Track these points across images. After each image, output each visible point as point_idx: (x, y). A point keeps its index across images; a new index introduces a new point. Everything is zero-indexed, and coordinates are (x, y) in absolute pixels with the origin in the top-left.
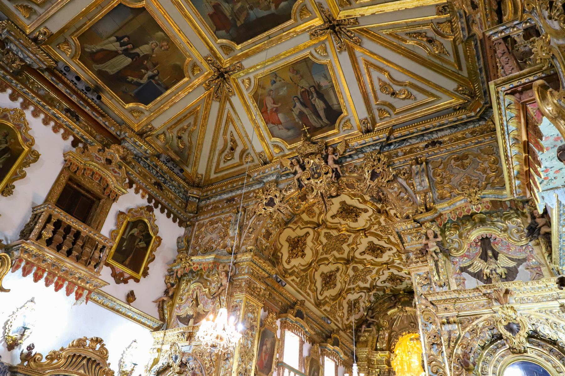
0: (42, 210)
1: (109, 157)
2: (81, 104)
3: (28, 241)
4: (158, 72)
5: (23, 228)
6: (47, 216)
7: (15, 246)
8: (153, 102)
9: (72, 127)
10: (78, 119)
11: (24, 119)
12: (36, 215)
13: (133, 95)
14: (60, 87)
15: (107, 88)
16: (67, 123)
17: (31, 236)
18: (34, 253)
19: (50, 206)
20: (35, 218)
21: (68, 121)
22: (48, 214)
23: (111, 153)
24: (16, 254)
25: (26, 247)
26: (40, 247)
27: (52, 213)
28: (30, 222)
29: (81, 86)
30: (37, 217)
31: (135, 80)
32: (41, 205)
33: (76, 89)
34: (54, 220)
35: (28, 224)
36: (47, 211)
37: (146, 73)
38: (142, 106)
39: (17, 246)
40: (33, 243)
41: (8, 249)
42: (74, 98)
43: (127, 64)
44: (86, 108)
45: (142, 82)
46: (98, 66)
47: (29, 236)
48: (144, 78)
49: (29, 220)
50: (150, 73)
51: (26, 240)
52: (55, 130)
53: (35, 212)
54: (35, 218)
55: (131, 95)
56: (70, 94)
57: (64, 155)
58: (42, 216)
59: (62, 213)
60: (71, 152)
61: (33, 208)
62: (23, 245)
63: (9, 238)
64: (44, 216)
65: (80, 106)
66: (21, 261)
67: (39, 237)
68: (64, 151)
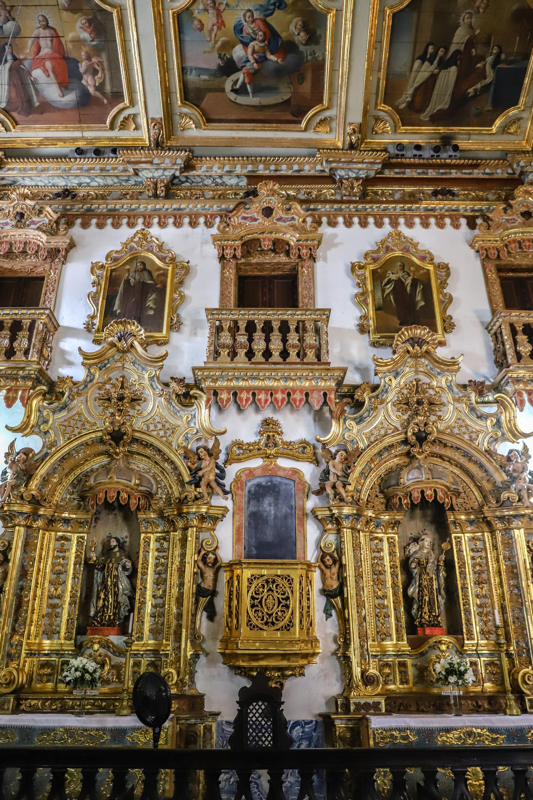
0: (498, 324)
1: (523, 209)
2: (443, 174)
3: (511, 368)
4: (499, 47)
5: (493, 357)
6: (508, 328)
7: (502, 380)
8: (523, 93)
9: (454, 207)
10: (453, 194)
11: (405, 238)
12: (495, 334)
13: (490, 108)
14: (410, 173)
15: (456, 129)
16: (446, 207)
17: (510, 361)
18: (528, 378)
19: (503, 314)
20: (497, 338)
21: (445, 205)
22: (508, 325)
23: (521, 202)
24: (509, 388)
25: (515, 376)
26: (528, 367)
27: (511, 321)
28: (495, 345)
29: (427, 153)
30: (499, 335)
31: (479, 86)
32: (492, 320)
33: (425, 161)
34: (519, 328)
35: (495, 349)
36: (503, 321)
37: (485, 66)
38: (513, 112)
39: (505, 380)
40: (518, 367)
41: (497, 388)
42: (432, 173)
43: (455, 78)
44: (451, 173)
45: (488, 80)
46: (426, 113)
47: (507, 361)
48: (488, 74)
49: (492, 344)
50: (490, 59)
51: (508, 367)
52: (441, 225)
53: (493, 332)
54: (497, 337)
55: (488, 111)
56: (423, 173)
57: (472, 246)
58: (503, 330)
59: (523, 315)
60: (477, 236)
61: (487, 328)
62: (510, 375)
63: (488, 376)
64: (506, 329)
65: (444, 177)
66: (520, 394)
67: (519, 357)
68: (467, 241)
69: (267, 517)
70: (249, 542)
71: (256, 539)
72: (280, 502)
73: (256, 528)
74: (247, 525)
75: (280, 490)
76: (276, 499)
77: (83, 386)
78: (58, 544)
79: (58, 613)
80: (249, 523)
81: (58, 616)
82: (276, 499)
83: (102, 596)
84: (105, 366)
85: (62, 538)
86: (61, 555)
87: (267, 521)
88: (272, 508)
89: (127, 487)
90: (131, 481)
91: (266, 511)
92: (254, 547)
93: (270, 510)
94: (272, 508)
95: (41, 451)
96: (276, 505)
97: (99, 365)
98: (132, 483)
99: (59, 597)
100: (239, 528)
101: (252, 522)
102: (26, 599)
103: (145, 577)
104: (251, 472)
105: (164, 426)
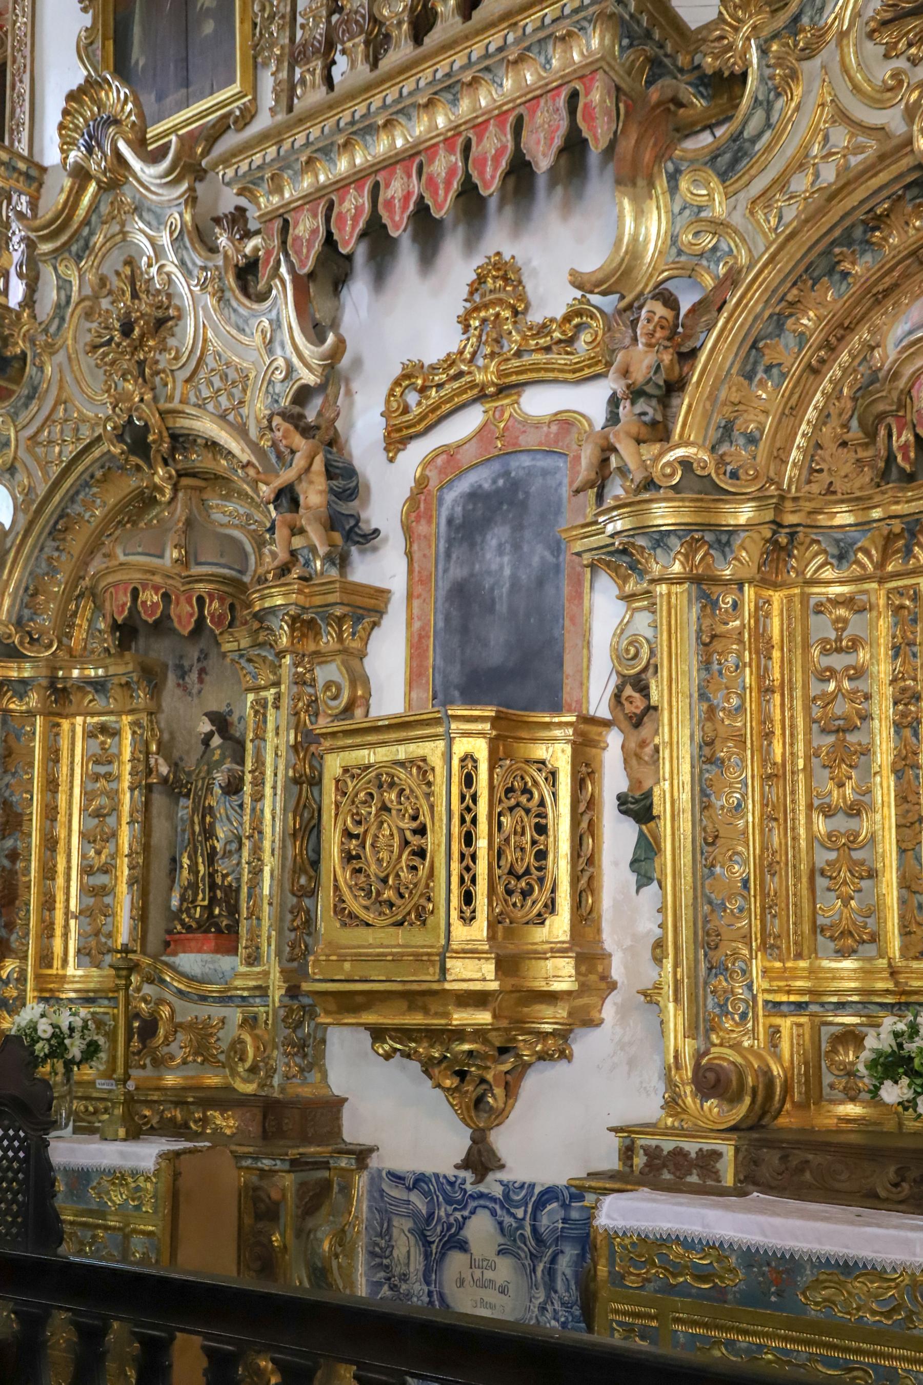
69: (492, 589)
70: (445, 676)
71: (463, 663)
72: (528, 534)
73: (464, 630)
74: (441, 624)
75: (527, 494)
76: (518, 527)
77: (56, 321)
78: (94, 746)
79: (108, 906)
80: (447, 619)
81: (108, 912)
82: (518, 527)
83: (186, 861)
84: (86, 246)
85: (104, 729)
86: (102, 770)
87: (493, 602)
88: (506, 559)
89: (153, 573)
90: (161, 556)
91: (489, 573)
92: (457, 687)
93: (501, 568)
94: (506, 559)
95: (14, 522)
96: (517, 547)
97: (74, 248)
98: (167, 562)
99: (106, 870)
100: (421, 637)
101: (454, 613)
102: (25, 879)
103: (259, 806)
104: (449, 452)
105: (224, 377)
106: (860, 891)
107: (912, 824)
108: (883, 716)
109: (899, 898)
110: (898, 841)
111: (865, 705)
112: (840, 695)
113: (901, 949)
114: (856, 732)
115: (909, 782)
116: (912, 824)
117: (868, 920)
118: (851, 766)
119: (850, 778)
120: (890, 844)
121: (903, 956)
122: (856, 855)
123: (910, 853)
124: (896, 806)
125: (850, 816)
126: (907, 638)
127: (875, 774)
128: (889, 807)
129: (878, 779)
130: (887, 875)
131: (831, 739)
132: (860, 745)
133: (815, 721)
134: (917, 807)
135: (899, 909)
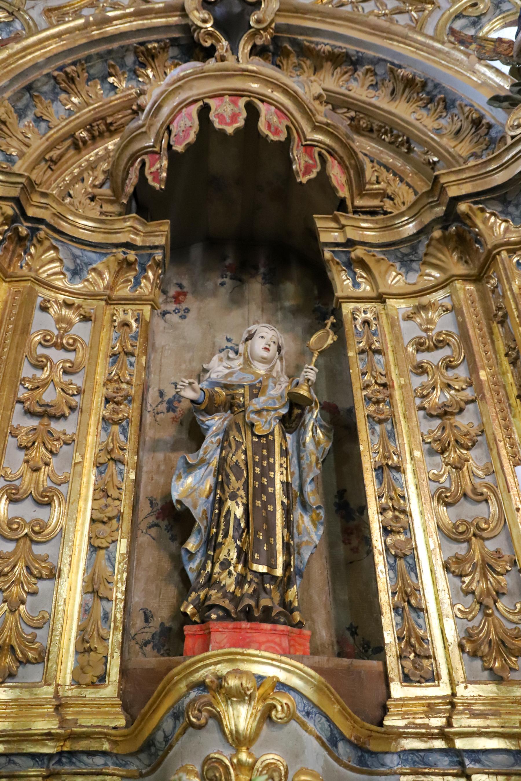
106: (34, 594)
107: (110, 519)
108: (93, 412)
109: (81, 606)
110: (90, 538)
111: (77, 398)
112: (51, 385)
113: (73, 673)
114: (62, 421)
115: (112, 476)
116: (110, 519)
117: (37, 631)
118: (51, 452)
119: (47, 464)
120: (81, 540)
121: (76, 682)
122: (38, 550)
123: (103, 552)
124: (94, 500)
125: (39, 504)
126: (127, 348)
127: (76, 464)
128: (86, 500)
129: (79, 468)
130: (72, 576)
131: (34, 423)
132: (65, 434)
133: (20, 402)
134: (117, 503)
135: (79, 620)
